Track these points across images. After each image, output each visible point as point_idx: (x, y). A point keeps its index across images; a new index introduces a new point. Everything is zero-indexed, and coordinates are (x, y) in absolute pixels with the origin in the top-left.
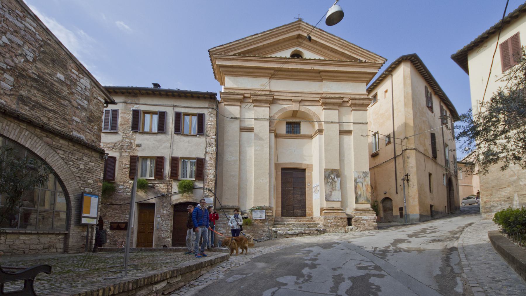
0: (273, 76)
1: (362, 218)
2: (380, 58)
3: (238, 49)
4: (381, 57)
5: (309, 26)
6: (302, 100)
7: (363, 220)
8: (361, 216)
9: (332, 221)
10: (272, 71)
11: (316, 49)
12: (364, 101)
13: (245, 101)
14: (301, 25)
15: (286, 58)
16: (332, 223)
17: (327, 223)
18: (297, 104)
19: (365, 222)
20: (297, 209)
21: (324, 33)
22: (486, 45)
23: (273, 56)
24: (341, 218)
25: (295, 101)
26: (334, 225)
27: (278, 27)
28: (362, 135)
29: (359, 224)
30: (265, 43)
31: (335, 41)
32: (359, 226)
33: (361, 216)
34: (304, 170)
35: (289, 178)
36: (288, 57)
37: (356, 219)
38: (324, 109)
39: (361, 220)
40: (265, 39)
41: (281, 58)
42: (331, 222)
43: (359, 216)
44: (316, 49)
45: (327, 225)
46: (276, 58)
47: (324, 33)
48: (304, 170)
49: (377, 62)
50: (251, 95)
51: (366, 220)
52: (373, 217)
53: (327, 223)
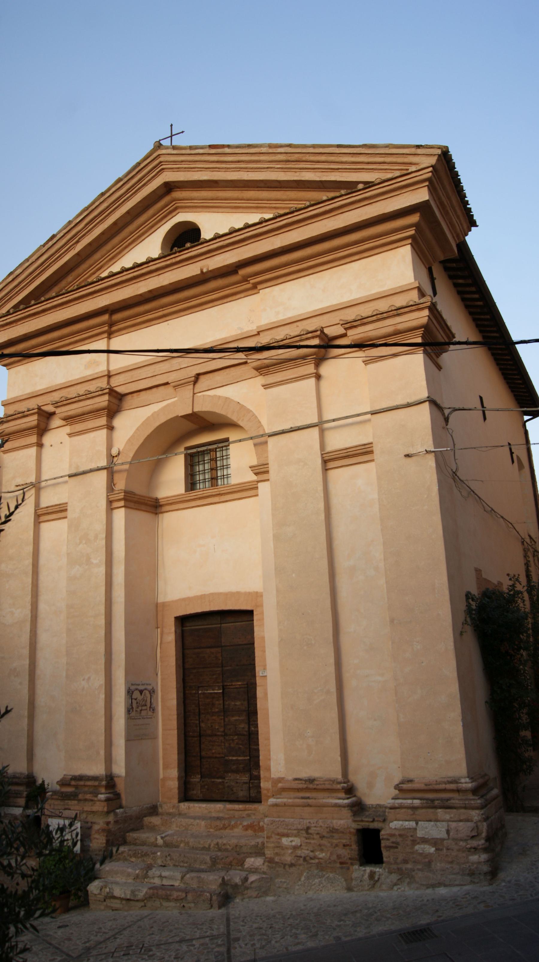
0: (114, 328)
1: (420, 834)
2: (419, 151)
3: (18, 293)
4: (418, 147)
5: (183, 152)
6: (198, 377)
7: (424, 841)
8: (412, 824)
9: (297, 841)
10: (106, 317)
11: (226, 199)
12: (398, 319)
13: (49, 428)
14: (162, 159)
15: (150, 261)
16: (299, 852)
17: (277, 850)
18: (187, 391)
19: (433, 850)
20: (237, 771)
21: (227, 150)
22: (232, 229)
23: (116, 268)
24: (333, 831)
25: (179, 385)
26: (305, 859)
27: (103, 194)
28: (407, 456)
29: (406, 861)
30: (79, 247)
31: (262, 158)
32: (404, 867)
33: (412, 824)
34: (250, 613)
35: (208, 650)
36: (156, 256)
37: (392, 835)
38: (266, 386)
39: (415, 842)
40: (77, 238)
41: (137, 266)
42: (295, 848)
43: (407, 824)
44: (226, 199)
45: (277, 859)
46: (124, 270)
47: (227, 150)
48: (250, 613)
49: (413, 168)
50: (57, 404)
51: (436, 843)
52: (464, 828)
53: (277, 850)
